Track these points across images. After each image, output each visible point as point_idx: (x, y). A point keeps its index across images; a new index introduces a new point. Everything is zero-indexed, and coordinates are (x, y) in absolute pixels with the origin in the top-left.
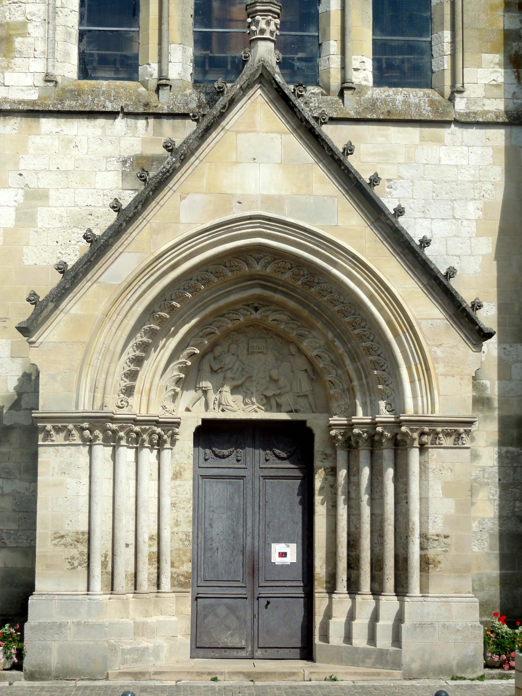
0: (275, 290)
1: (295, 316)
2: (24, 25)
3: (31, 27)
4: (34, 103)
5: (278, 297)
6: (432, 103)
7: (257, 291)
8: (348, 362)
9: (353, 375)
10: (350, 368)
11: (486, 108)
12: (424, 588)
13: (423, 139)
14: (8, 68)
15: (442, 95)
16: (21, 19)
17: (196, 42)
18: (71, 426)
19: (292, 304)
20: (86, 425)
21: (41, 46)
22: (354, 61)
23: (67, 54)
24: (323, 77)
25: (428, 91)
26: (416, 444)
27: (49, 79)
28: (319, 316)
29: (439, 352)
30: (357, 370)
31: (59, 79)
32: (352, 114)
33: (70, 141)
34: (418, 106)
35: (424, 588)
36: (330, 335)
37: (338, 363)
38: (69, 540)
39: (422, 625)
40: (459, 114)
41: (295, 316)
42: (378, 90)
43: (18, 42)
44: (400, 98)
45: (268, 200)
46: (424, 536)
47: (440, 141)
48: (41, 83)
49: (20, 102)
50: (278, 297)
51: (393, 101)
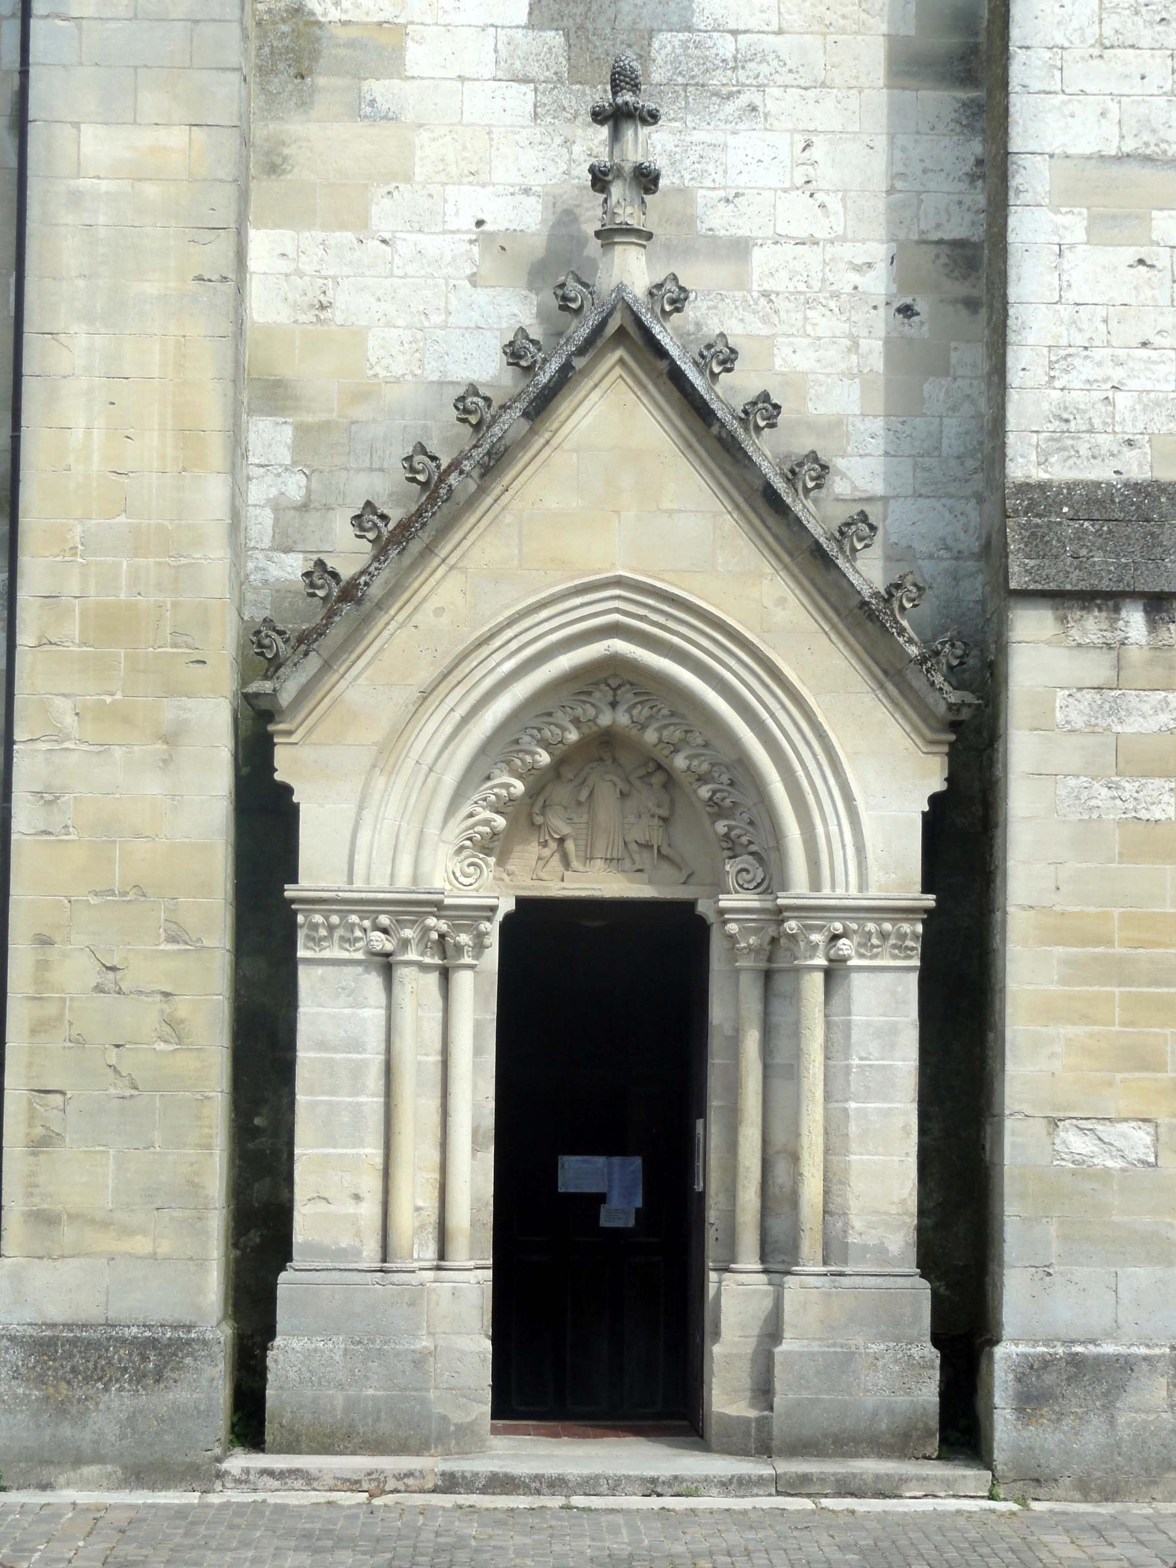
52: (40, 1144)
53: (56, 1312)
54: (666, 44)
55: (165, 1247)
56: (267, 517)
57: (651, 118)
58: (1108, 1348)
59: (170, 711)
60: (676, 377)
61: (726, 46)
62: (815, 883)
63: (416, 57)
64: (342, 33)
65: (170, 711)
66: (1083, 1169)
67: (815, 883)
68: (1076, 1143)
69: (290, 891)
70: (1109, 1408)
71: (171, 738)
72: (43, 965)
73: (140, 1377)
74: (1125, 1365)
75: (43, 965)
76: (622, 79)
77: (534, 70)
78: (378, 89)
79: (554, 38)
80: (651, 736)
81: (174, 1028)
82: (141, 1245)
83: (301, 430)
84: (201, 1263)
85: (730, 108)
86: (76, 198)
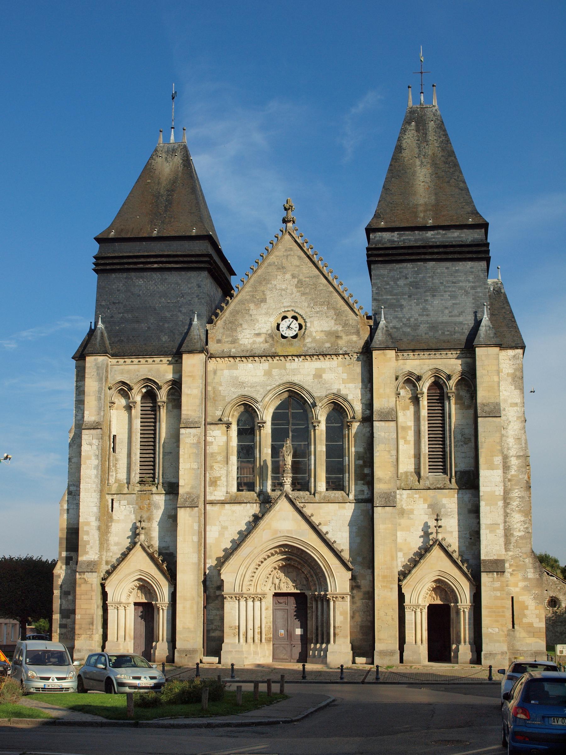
0: (293, 556)
1: (299, 563)
2: (220, 477)
3: (222, 478)
4: (223, 500)
5: (294, 557)
6: (342, 496)
7: (288, 556)
8: (314, 576)
9: (316, 580)
10: (315, 578)
11: (359, 498)
12: (334, 642)
13: (339, 508)
14: (215, 490)
15: (346, 493)
16: (219, 475)
17: (272, 479)
18: (233, 596)
19: (298, 560)
20: (237, 596)
21: (225, 483)
22: (318, 484)
23: (233, 485)
24: (310, 489)
25: (342, 492)
26: (332, 600)
27: (227, 493)
28: (305, 563)
29: (338, 574)
30: (317, 578)
31: (231, 493)
32: (317, 501)
33: (234, 511)
34: (338, 498)
35: (334, 642)
36: (309, 569)
37: (312, 576)
38: (233, 628)
39: (333, 652)
40: (351, 500)
41: (299, 563)
42: (327, 492)
43: (218, 482)
44: (333, 495)
45: (288, 531)
46: (334, 627)
47: (344, 508)
48: (225, 494)
49: (219, 500)
50: (294, 557)
51: (330, 496)
52: (378, 632)
53: (381, 649)
54: (443, 510)
55: (392, 642)
56: (400, 563)
57: (441, 520)
58: (494, 652)
59: (391, 586)
60: (445, 548)
61: (450, 510)
62: (461, 603)
63: (415, 512)
64: (407, 510)
65: (391, 586)
66: (491, 633)
67: (461, 603)
68: (490, 630)
69: (404, 604)
70: (494, 659)
71: (391, 589)
72: (378, 613)
73: (390, 655)
74: (496, 654)
75: (378, 613)
76: (437, 515)
77: (428, 513)
78: (411, 516)
79: (430, 510)
80: (443, 587)
81: (393, 619)
82: (390, 642)
83: (404, 553)
84: (396, 644)
85: (450, 517)
86: (379, 532)
